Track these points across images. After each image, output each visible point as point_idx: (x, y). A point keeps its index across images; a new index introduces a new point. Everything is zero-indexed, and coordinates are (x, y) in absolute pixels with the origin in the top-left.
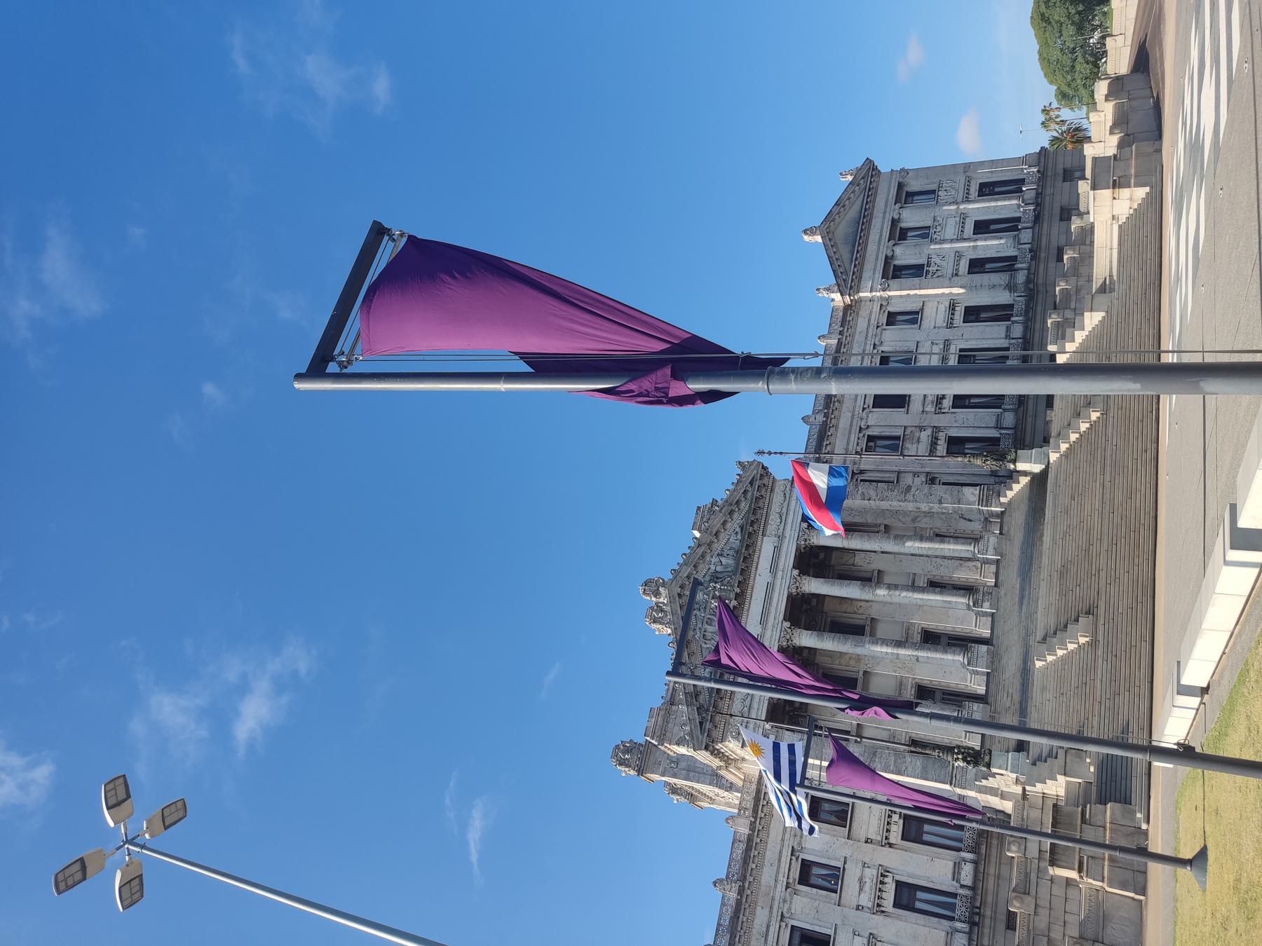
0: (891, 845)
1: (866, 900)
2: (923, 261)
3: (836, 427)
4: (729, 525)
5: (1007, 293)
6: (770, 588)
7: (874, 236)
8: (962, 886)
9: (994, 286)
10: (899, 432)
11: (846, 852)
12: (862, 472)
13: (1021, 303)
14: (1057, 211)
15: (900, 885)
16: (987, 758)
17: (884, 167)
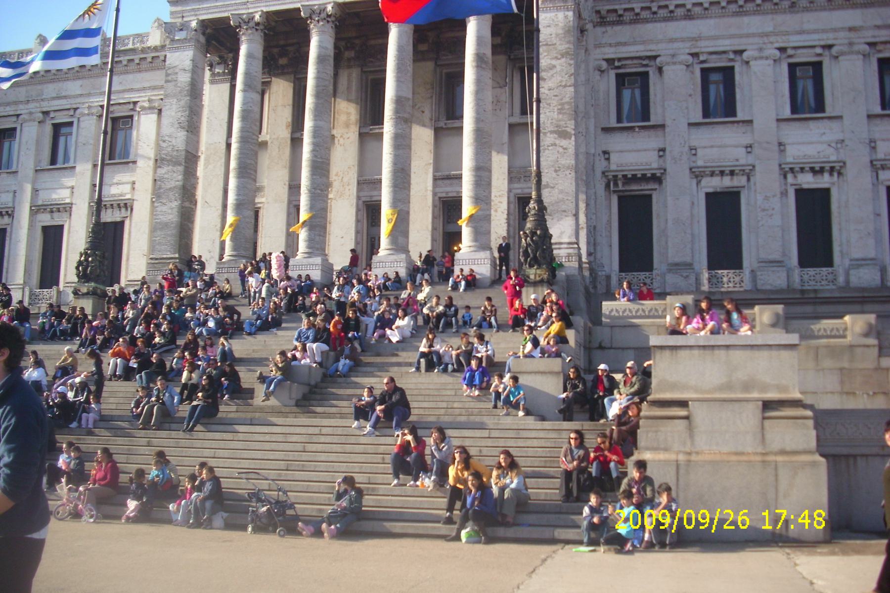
10: (740, 116)
12: (660, 70)
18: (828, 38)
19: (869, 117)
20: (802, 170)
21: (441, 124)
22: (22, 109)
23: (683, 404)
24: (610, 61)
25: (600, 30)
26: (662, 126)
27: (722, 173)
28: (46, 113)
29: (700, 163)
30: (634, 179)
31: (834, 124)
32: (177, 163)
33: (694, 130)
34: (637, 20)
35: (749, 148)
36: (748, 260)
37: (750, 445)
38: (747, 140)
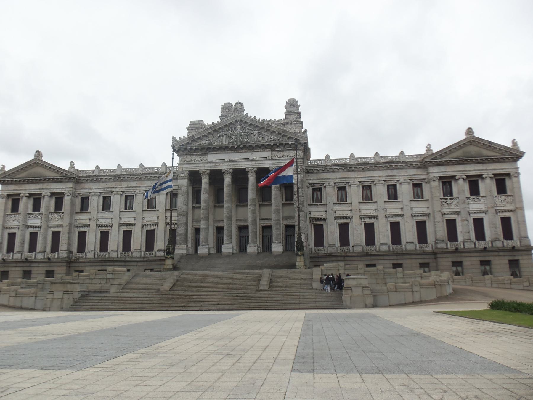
0: (166, 226)
1: (146, 220)
2: (455, 195)
3: (348, 171)
4: (275, 134)
5: (434, 240)
6: (247, 160)
7: (469, 167)
8: (155, 252)
9: (436, 233)
11: (160, 211)
12: (325, 187)
13: (428, 248)
14: (487, 259)
15: (154, 230)
16: (169, 257)
17: (520, 163)
18: (373, 179)
19: (385, 202)
20: (366, 217)
21: (261, 203)
22: (113, 190)
23: (351, 287)
24: (310, 184)
25: (307, 175)
26: (326, 204)
27: (343, 218)
28: (123, 192)
29: (337, 215)
30: (318, 220)
31: (375, 204)
32: (183, 215)
33: (335, 205)
34: (318, 172)
35: (351, 211)
36: (351, 243)
37: (361, 293)
38: (350, 208)
